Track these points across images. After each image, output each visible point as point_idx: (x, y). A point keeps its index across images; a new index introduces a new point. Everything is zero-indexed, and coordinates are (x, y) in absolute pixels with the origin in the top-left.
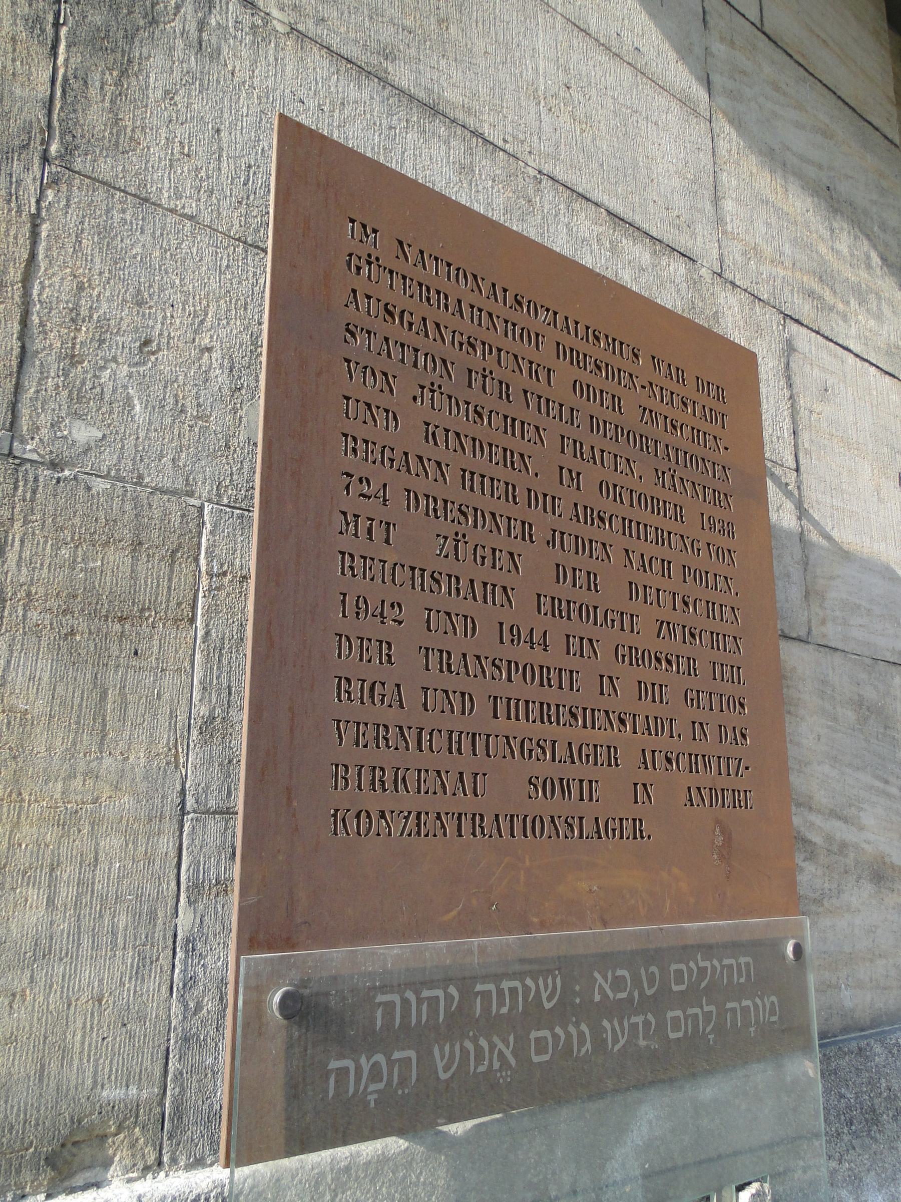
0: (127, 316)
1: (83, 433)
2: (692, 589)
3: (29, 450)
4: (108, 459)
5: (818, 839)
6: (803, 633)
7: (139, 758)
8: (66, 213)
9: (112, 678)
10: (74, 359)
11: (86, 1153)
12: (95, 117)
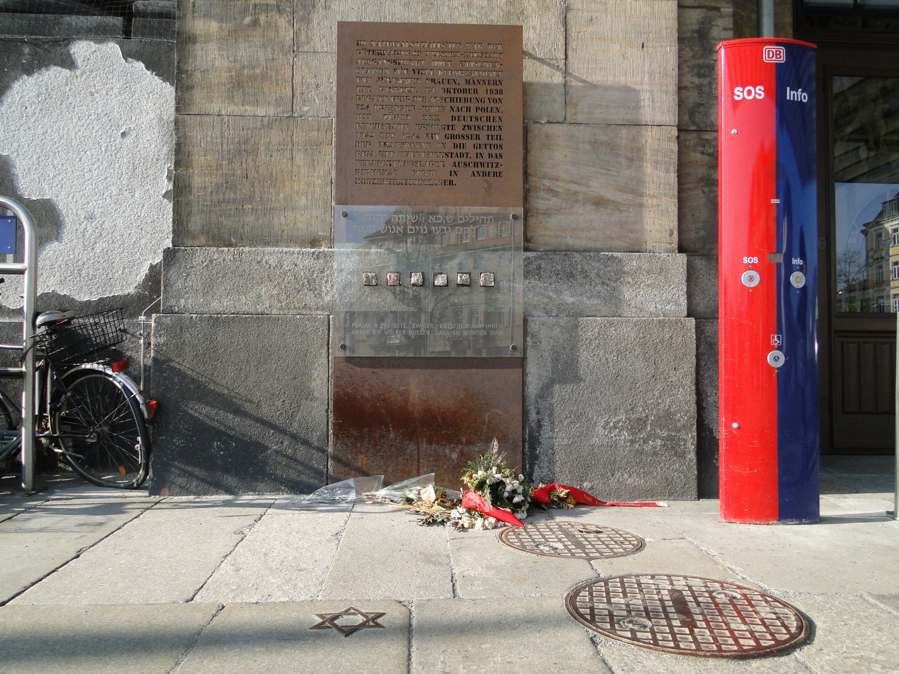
0: (313, 81)
1: (306, 109)
2: (480, 114)
3: (296, 115)
4: (311, 113)
5: (561, 190)
6: (561, 120)
7: (322, 172)
8: (299, 62)
9: (315, 158)
10: (303, 94)
11: (317, 243)
12: (303, 37)
